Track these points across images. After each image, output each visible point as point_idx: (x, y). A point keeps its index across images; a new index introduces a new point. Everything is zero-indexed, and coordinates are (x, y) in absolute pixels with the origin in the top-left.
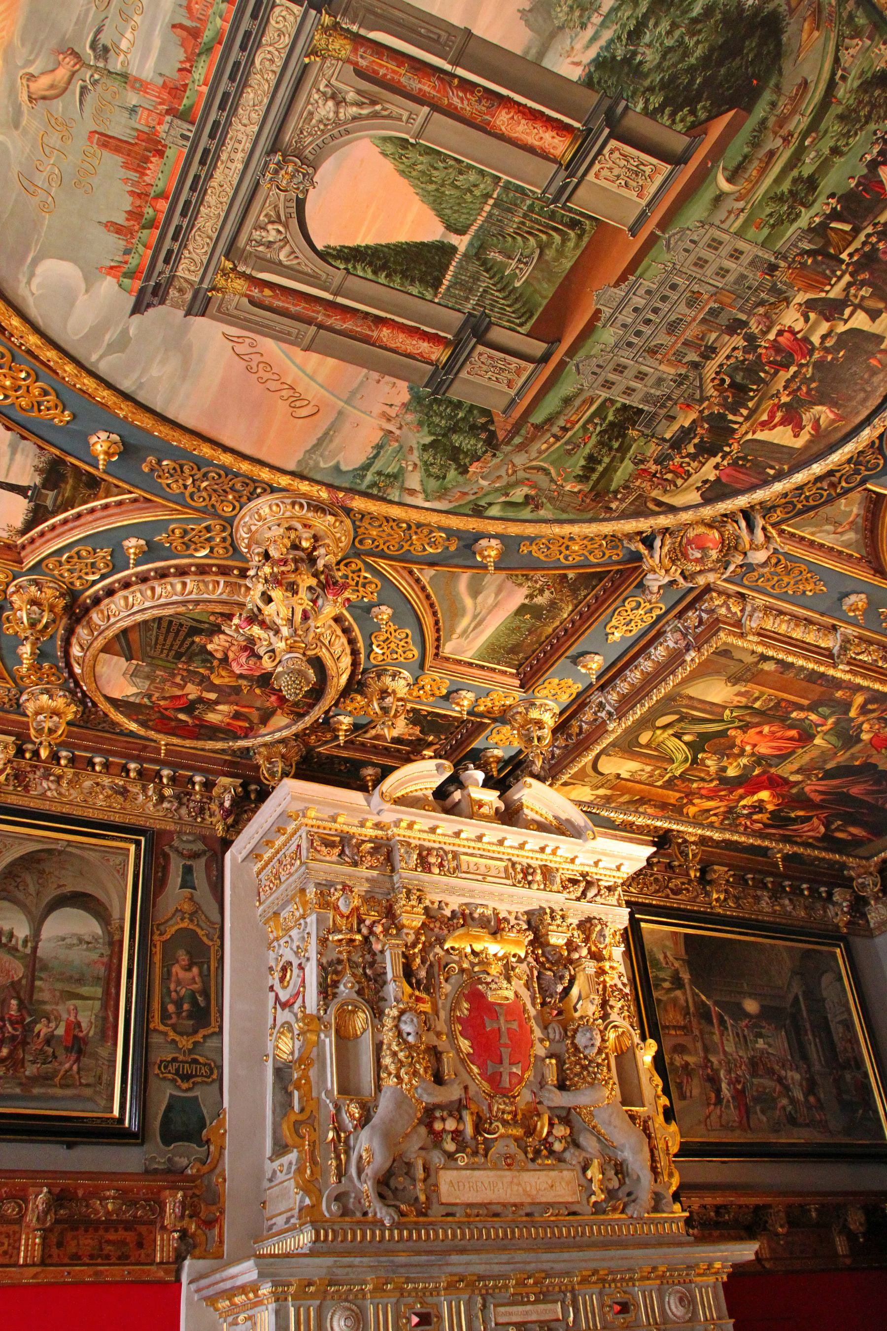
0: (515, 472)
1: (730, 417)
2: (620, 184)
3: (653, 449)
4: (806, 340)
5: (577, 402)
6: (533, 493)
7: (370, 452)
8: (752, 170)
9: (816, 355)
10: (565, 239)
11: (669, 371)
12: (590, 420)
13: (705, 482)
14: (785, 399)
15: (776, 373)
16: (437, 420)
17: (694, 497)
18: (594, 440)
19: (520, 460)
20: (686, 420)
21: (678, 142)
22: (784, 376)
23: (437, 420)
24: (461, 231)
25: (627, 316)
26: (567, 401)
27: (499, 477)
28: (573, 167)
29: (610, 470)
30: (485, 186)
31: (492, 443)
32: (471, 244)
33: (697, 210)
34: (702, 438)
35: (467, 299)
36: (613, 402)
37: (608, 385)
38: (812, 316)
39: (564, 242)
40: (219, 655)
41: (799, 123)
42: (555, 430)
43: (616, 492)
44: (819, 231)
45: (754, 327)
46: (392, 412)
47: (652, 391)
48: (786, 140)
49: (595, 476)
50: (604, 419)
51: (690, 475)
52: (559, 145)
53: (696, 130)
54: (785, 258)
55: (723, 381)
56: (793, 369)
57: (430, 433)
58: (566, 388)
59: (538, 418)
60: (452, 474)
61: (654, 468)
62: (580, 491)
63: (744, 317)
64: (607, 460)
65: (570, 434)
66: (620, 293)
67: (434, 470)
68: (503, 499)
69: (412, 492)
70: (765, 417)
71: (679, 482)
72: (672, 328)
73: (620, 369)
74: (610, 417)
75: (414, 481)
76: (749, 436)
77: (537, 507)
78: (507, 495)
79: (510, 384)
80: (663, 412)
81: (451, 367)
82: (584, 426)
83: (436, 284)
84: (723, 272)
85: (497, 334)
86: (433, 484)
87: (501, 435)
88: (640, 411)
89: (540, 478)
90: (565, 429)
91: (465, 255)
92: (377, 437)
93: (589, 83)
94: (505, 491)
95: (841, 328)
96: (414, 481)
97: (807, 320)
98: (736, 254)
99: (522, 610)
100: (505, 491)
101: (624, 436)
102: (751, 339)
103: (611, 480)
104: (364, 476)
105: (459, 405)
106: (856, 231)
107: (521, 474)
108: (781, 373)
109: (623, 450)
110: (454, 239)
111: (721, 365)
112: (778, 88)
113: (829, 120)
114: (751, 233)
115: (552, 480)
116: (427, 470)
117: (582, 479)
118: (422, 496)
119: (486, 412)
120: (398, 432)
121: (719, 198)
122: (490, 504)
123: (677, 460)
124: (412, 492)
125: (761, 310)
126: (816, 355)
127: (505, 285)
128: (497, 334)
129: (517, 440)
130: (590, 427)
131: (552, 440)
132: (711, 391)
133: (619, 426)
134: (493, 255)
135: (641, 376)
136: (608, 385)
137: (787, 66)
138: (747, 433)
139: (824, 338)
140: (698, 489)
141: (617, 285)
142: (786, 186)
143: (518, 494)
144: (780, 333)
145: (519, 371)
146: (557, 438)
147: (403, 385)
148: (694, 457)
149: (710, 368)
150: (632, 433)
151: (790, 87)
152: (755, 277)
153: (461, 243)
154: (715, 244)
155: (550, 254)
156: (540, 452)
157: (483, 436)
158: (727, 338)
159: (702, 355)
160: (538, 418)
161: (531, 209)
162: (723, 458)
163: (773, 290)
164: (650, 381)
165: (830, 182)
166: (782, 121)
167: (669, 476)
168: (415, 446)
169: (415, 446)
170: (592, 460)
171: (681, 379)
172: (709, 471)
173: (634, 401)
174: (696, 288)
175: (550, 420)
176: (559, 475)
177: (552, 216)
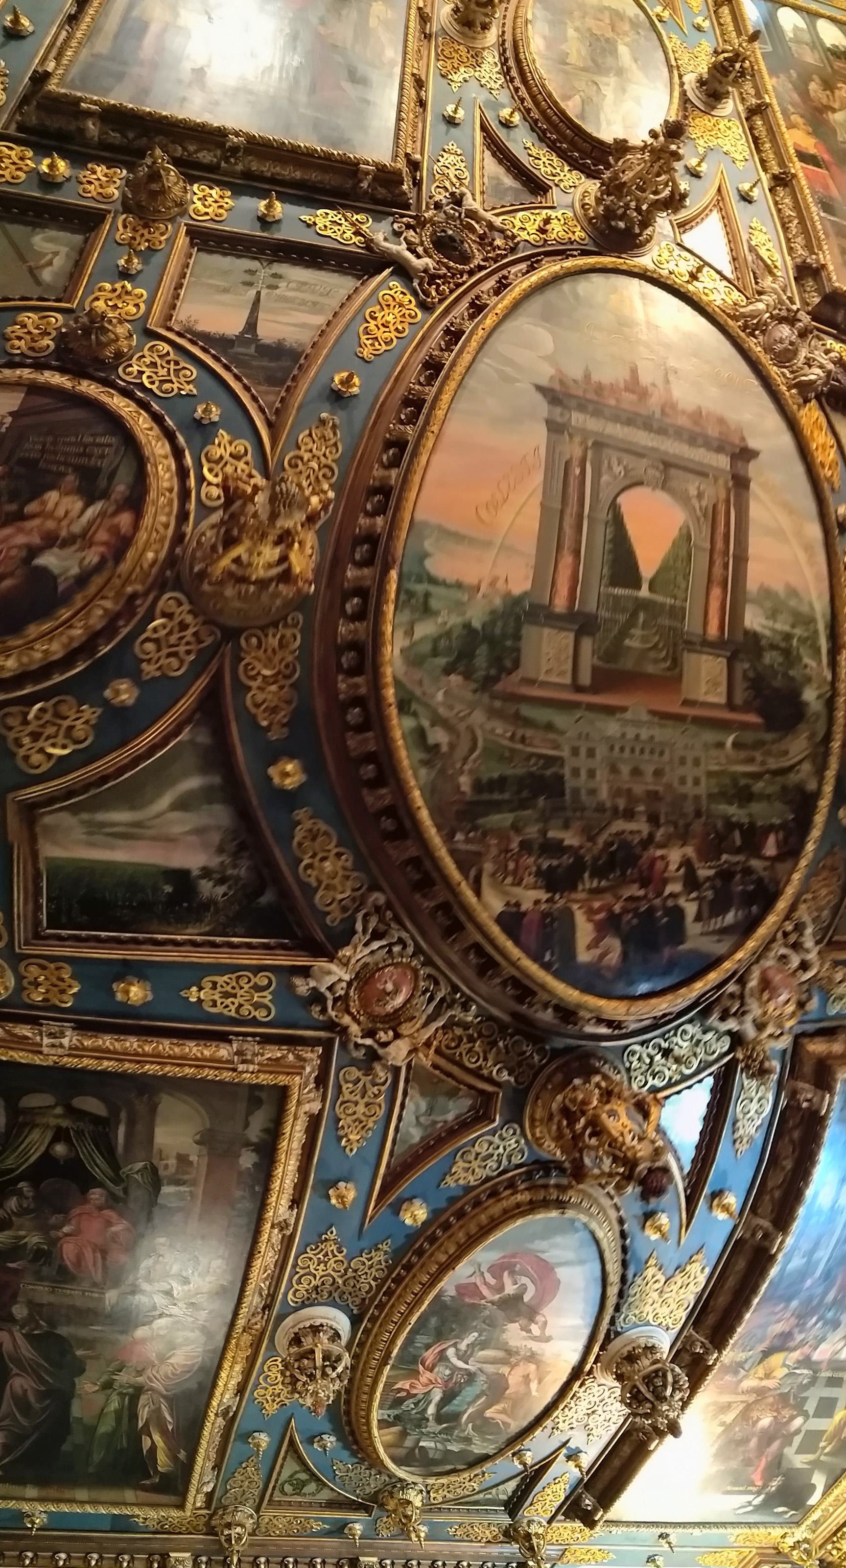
0: (463, 719)
1: (586, 875)
2: (707, 678)
3: (532, 831)
4: (665, 882)
5: (551, 736)
6: (444, 749)
7: (451, 578)
8: (743, 754)
9: (658, 902)
10: (664, 659)
11: (604, 794)
12: (540, 756)
13: (518, 905)
14: (617, 908)
15: (634, 882)
16: (499, 624)
17: (497, 905)
18: (520, 771)
19: (478, 717)
20: (571, 839)
21: (739, 699)
22: (635, 890)
23: (499, 624)
24: (651, 588)
25: (631, 733)
26: (549, 727)
27: (451, 708)
28: (706, 645)
29: (496, 807)
30: (680, 594)
31: (487, 684)
32: (644, 599)
33: (709, 736)
34: (558, 866)
35: (607, 610)
36: (562, 766)
37: (575, 752)
38: (682, 871)
39: (664, 659)
40: (32, 507)
41: (773, 764)
42: (520, 732)
43: (475, 828)
44: (731, 825)
45: (659, 834)
46: (500, 585)
47: (583, 793)
48: (763, 763)
49: (486, 797)
50: (546, 767)
51: (519, 884)
52: (713, 630)
53: (746, 708)
54: (708, 817)
55: (612, 844)
56: (641, 893)
57: (484, 626)
58: (560, 720)
59: (526, 711)
60: (442, 661)
61: (515, 845)
62: (464, 793)
63: (662, 820)
64: (506, 796)
65: (519, 746)
66: (645, 717)
67: (443, 643)
68: (426, 723)
69: (410, 632)
70: (597, 905)
71: (509, 880)
72: (636, 772)
73: (591, 753)
74: (548, 772)
75: (425, 629)
76: (575, 907)
77: (426, 763)
78: (433, 725)
79: (548, 672)
80: (569, 814)
81: (551, 619)
82: (532, 755)
83: (613, 583)
84: (683, 781)
85: (587, 644)
86: (427, 648)
87: (499, 687)
88: (562, 794)
89: (464, 746)
90: (523, 740)
91: (637, 598)
92: (470, 579)
93: (746, 633)
94: (438, 721)
95: (682, 902)
96: (425, 629)
97: (678, 869)
98: (697, 782)
99: (181, 879)
100: (438, 721)
101: (535, 796)
102: (651, 836)
103: (486, 814)
104: (419, 580)
105: (517, 637)
106: (738, 851)
107: (462, 727)
108: (636, 886)
109: (523, 805)
110: (645, 587)
111: (623, 832)
112: (780, 740)
113: (779, 779)
114: (713, 781)
115: (465, 760)
116: (440, 637)
117: (478, 786)
118: (407, 643)
119: (516, 664)
120: (480, 594)
121: (721, 745)
122: (415, 715)
123: (531, 860)
124: (410, 632)
125: (671, 829)
126: (658, 902)
127: (624, 633)
128: (587, 644)
129: (498, 704)
130: (533, 761)
131: (509, 734)
132: (601, 840)
133: (542, 786)
134: (641, 617)
135: (591, 774)
136: (575, 752)
137: (790, 737)
138: (577, 901)
139: (671, 895)
140: (508, 904)
141: (653, 713)
142: (743, 782)
143: (438, 736)
144: (662, 857)
145: (562, 674)
146: (512, 738)
147: (527, 586)
148: (539, 873)
149: (619, 825)
150: (541, 802)
151: (782, 746)
152: (689, 808)
153: (644, 592)
154: (697, 762)
155: (652, 654)
156: (493, 730)
157: (493, 672)
158: (644, 818)
159: (625, 810)
160: (526, 711)
161: (675, 629)
162: (547, 901)
163: (688, 826)
164: (591, 785)
165: (756, 808)
166: (768, 753)
167: (511, 866)
168: (468, 615)
169: (468, 615)
170: (501, 783)
171: (600, 808)
172: (530, 897)
173: (570, 783)
174: (667, 769)
175: (528, 722)
176: (475, 761)
177: (675, 645)
